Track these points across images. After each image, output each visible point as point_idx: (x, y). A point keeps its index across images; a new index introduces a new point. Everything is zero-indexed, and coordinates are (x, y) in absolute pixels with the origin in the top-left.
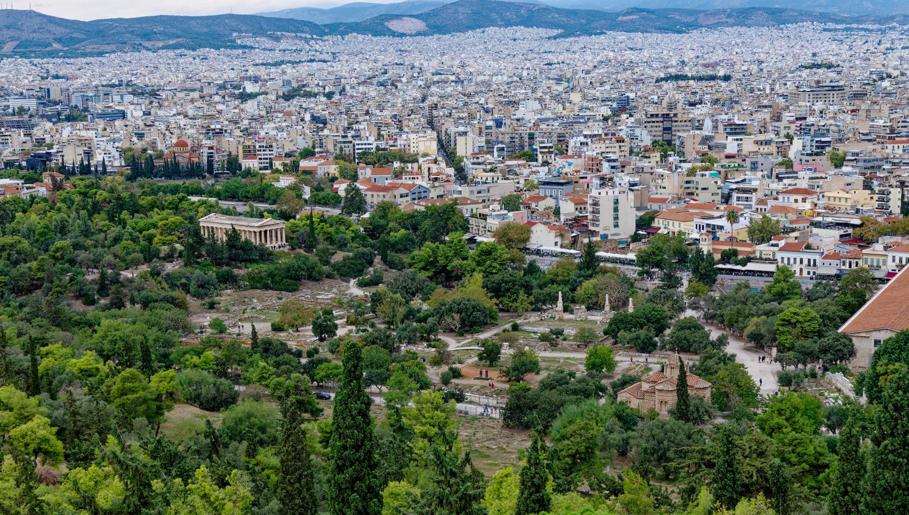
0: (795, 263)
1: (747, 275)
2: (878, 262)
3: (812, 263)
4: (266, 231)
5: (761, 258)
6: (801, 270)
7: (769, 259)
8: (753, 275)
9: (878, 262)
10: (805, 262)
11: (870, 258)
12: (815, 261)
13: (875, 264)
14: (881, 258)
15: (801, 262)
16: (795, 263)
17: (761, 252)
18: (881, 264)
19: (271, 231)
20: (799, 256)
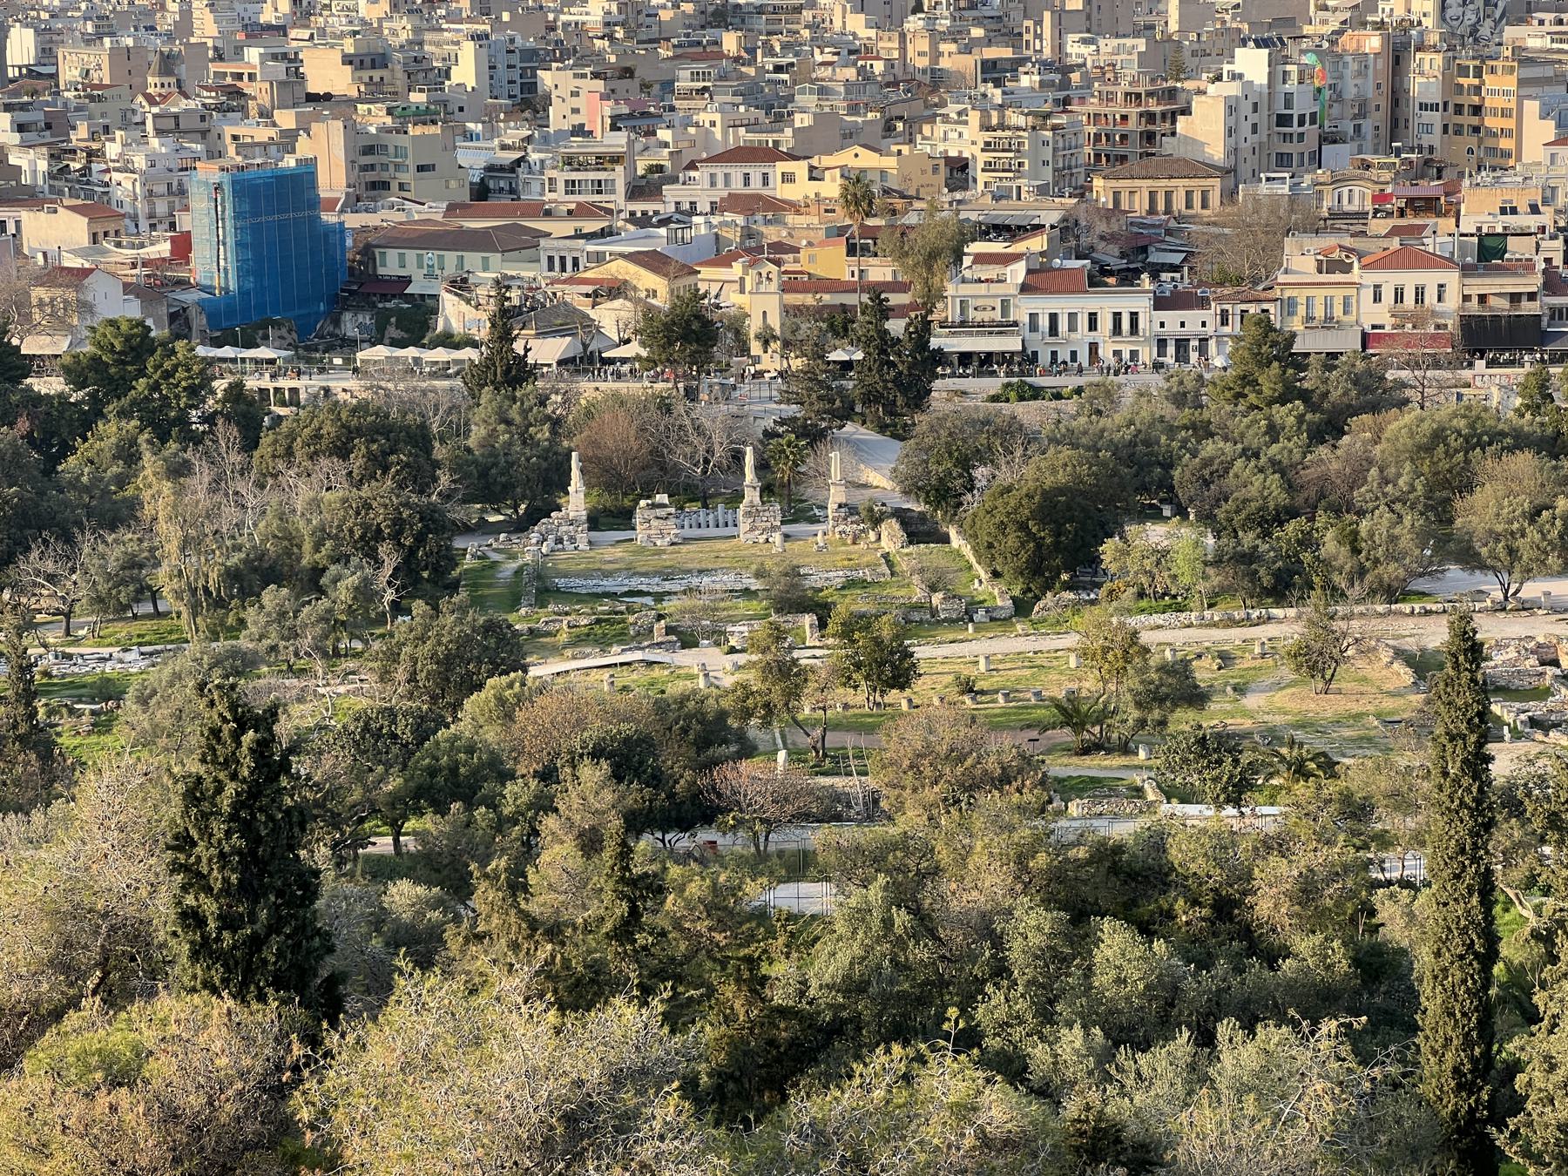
0: (1072, 328)
2: (1328, 304)
5: (963, 324)
6: (1093, 348)
7: (993, 324)
9: (1328, 304)
10: (1106, 323)
11: (1301, 295)
12: (1134, 316)
13: (1319, 312)
14: (1338, 295)
15: (1093, 325)
16: (1072, 328)
17: (964, 305)
18: (1338, 311)
20: (1083, 304)
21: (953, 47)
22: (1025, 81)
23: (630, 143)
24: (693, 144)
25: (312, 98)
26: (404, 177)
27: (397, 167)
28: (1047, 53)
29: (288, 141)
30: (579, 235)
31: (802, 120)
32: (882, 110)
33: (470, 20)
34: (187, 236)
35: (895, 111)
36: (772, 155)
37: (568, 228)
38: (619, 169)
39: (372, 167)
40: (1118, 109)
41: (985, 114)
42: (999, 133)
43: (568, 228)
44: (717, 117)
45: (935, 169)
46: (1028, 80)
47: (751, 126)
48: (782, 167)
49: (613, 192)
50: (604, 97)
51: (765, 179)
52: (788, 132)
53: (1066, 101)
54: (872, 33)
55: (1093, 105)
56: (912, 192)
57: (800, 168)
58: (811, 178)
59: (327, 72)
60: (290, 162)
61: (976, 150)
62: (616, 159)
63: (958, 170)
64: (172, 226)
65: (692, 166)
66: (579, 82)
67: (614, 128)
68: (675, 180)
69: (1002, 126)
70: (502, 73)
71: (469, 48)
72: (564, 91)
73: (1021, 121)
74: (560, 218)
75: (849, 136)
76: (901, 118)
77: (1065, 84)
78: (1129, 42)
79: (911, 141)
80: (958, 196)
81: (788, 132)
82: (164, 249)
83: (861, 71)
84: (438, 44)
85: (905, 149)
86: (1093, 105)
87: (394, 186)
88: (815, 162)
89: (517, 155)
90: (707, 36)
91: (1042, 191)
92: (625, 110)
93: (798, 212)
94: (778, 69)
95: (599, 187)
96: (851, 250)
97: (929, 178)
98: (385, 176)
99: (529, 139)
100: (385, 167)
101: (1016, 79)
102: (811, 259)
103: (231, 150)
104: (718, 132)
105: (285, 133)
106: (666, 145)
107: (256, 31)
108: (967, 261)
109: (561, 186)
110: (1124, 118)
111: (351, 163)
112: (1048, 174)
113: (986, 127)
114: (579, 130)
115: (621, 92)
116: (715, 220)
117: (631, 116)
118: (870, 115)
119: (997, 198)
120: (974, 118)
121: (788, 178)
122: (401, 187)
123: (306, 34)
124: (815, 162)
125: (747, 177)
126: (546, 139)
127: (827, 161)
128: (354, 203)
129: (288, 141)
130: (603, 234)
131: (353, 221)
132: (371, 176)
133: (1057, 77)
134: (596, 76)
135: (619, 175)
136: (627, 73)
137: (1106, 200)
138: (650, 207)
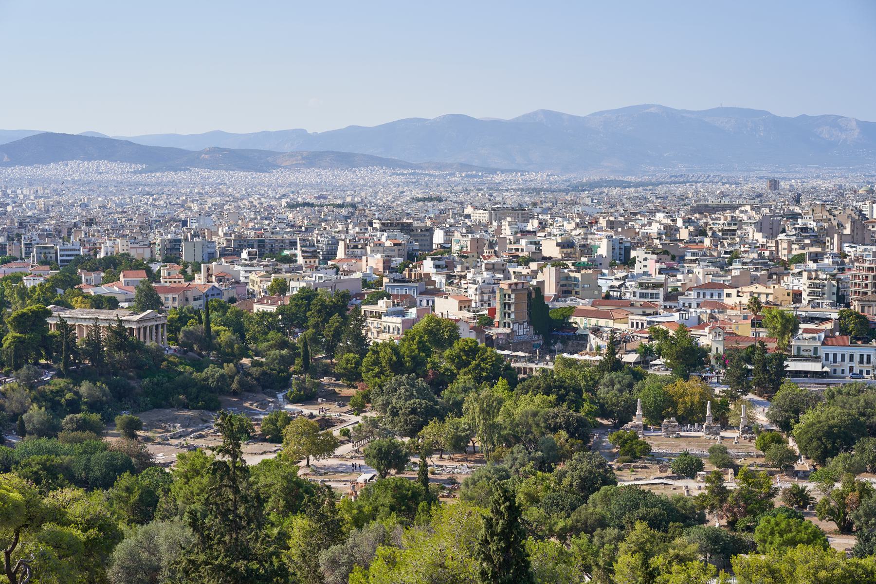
1: (796, 376)
3: (865, 360)
4: (157, 326)
8: (806, 377)
19: (145, 328)
21: (797, 247)
22: (826, 261)
23: (666, 279)
24: (691, 280)
25: (544, 258)
26: (577, 289)
27: (575, 285)
28: (836, 251)
29: (534, 274)
30: (644, 314)
31: (735, 273)
32: (768, 270)
33: (606, 231)
34: (495, 309)
35: (773, 271)
36: (722, 286)
37: (640, 311)
38: (661, 289)
39: (565, 285)
40: (864, 273)
41: (809, 272)
42: (816, 281)
43: (640, 311)
44: (701, 271)
45: (788, 294)
46: (827, 261)
47: (715, 275)
48: (726, 291)
49: (658, 298)
50: (657, 261)
51: (719, 296)
52: (729, 278)
53: (843, 270)
54: (764, 240)
55: (854, 272)
56: (779, 303)
57: (734, 292)
58: (738, 296)
59: (550, 249)
60: (534, 282)
61: (805, 287)
62: (661, 285)
63: (797, 297)
64: (489, 305)
65: (690, 289)
66: (647, 255)
67: (660, 273)
68: (683, 294)
69: (816, 278)
70: (617, 250)
71: (605, 242)
72: (641, 259)
73: (824, 277)
74: (637, 307)
75: (754, 280)
76: (775, 274)
77: (843, 263)
78: (869, 247)
79: (779, 283)
80: (798, 305)
81: (729, 278)
82: (486, 312)
83: (760, 255)
84: (592, 239)
85: (777, 286)
86: (854, 272)
87: (573, 292)
88: (740, 289)
89: (621, 282)
90: (698, 239)
91: (831, 305)
92: (664, 266)
93: (732, 309)
94: (726, 253)
95: (652, 296)
96: (753, 325)
97: (786, 297)
98: (570, 289)
99: (626, 277)
100: (570, 285)
101: (822, 260)
102: (737, 328)
103: (513, 277)
104: (701, 276)
105: (533, 271)
106: (680, 281)
107: (525, 233)
108: (800, 331)
109: (638, 295)
110: (867, 277)
111: (557, 283)
112: (835, 298)
113: (810, 278)
114: (645, 273)
115: (663, 259)
116: (699, 310)
117: (666, 269)
118: (763, 272)
119: (813, 307)
120: (805, 274)
121: (729, 295)
122: (576, 293)
123: (543, 234)
124: (740, 289)
125: (712, 295)
126: (633, 277)
127: (745, 289)
128: (556, 299)
129: (534, 274)
130: (656, 314)
131: (558, 305)
132: (565, 288)
133: (839, 260)
134: (653, 253)
135: (661, 291)
136: (666, 252)
137: (858, 309)
138: (673, 304)
